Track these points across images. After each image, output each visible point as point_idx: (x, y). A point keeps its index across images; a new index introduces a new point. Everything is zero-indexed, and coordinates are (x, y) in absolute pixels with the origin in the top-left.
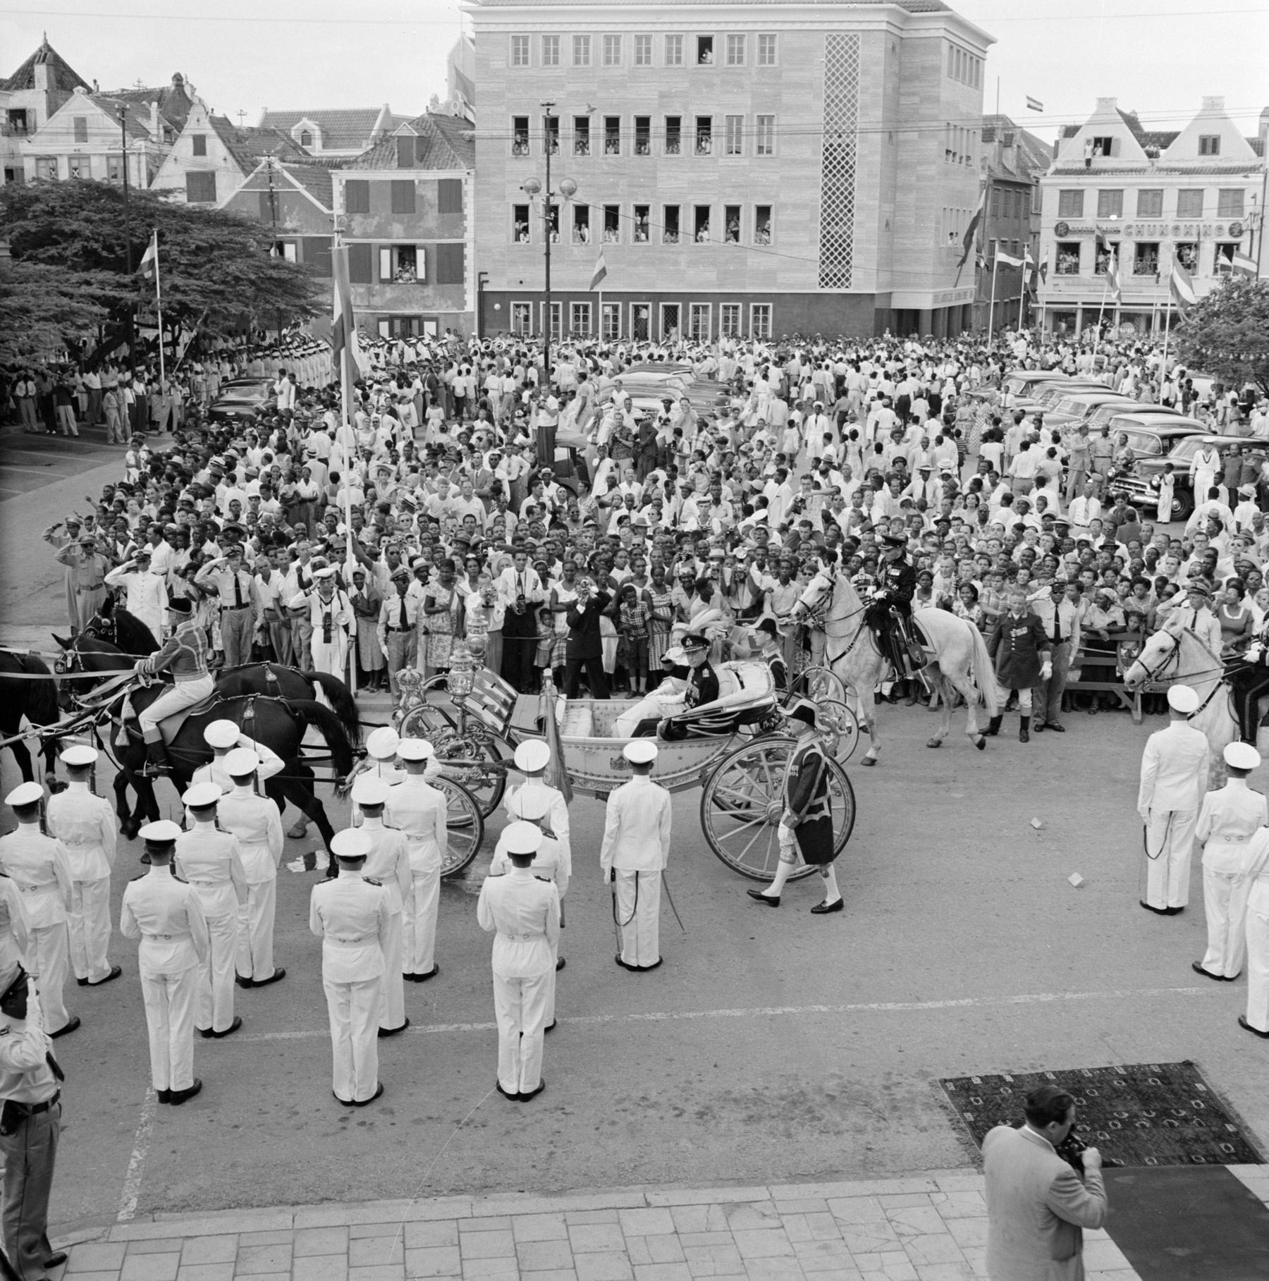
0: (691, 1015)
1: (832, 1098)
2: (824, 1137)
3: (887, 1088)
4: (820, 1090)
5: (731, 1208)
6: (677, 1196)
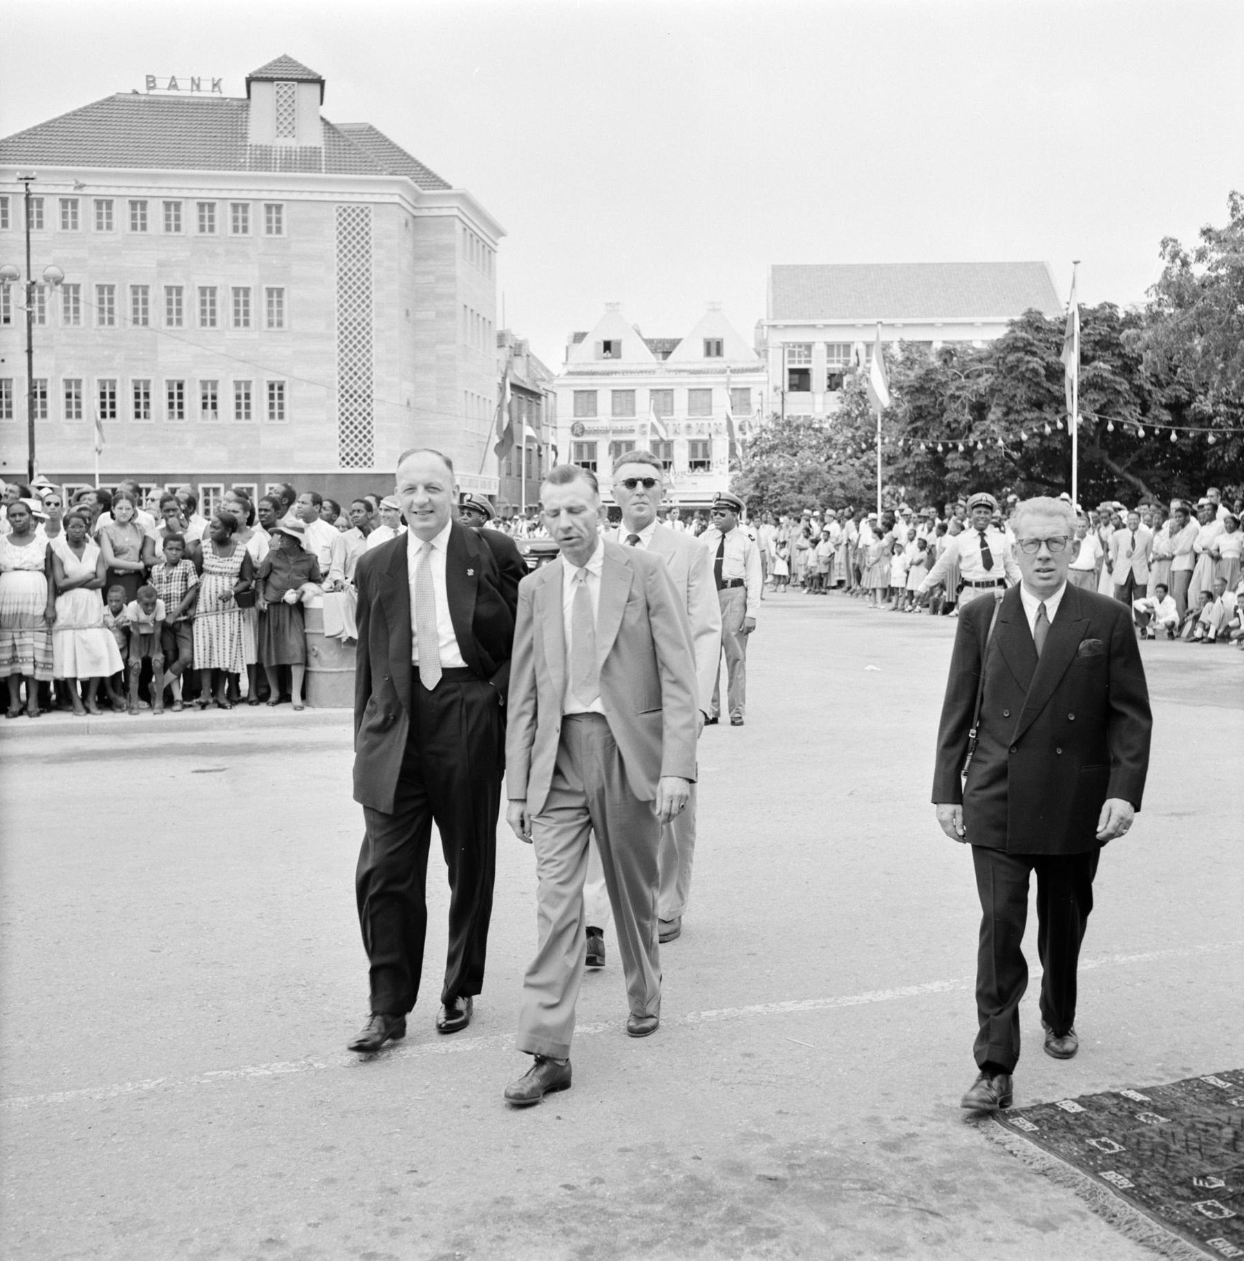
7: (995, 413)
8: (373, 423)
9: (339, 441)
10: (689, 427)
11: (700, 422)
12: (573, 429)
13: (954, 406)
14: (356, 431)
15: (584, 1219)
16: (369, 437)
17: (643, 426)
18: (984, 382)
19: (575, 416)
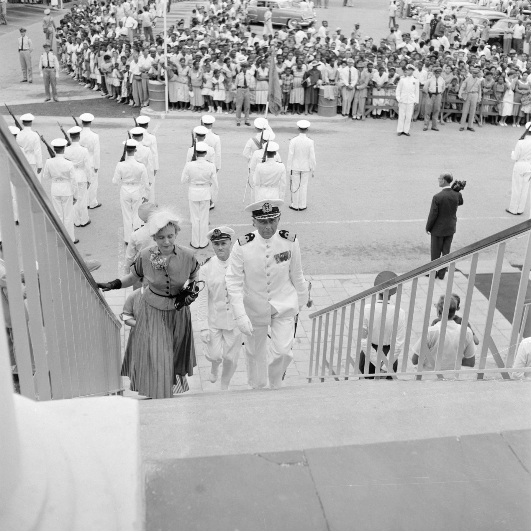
0: (319, 222)
1: (375, 249)
2: (373, 261)
3: (394, 246)
4: (370, 246)
5: (343, 281)
6: (322, 277)
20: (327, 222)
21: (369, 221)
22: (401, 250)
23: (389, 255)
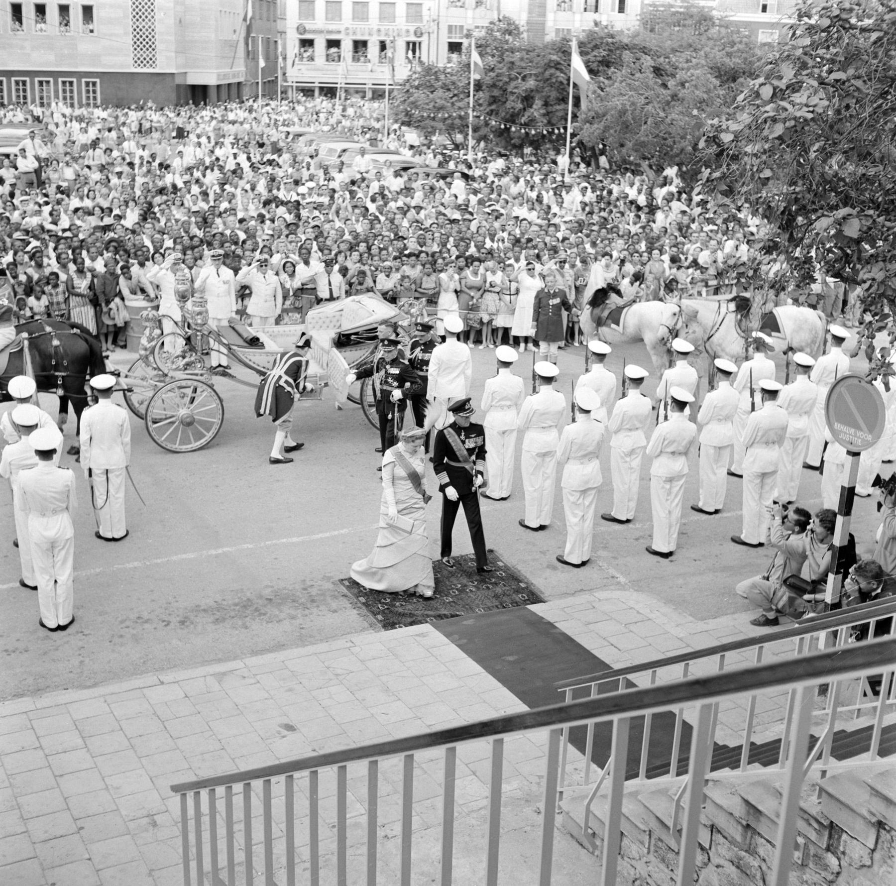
0: (159, 561)
1: (270, 600)
2: (270, 625)
3: (305, 589)
4: (261, 597)
6: (182, 675)
7: (538, 103)
8: (156, 37)
9: (132, 49)
10: (379, 30)
11: (387, 27)
12: (298, 28)
13: (512, 98)
14: (144, 42)
15: (218, 611)
16: (153, 46)
17: (347, 29)
18: (531, 83)
19: (300, 19)
20: (174, 558)
21: (250, 546)
22: (318, 594)
23: (296, 608)
